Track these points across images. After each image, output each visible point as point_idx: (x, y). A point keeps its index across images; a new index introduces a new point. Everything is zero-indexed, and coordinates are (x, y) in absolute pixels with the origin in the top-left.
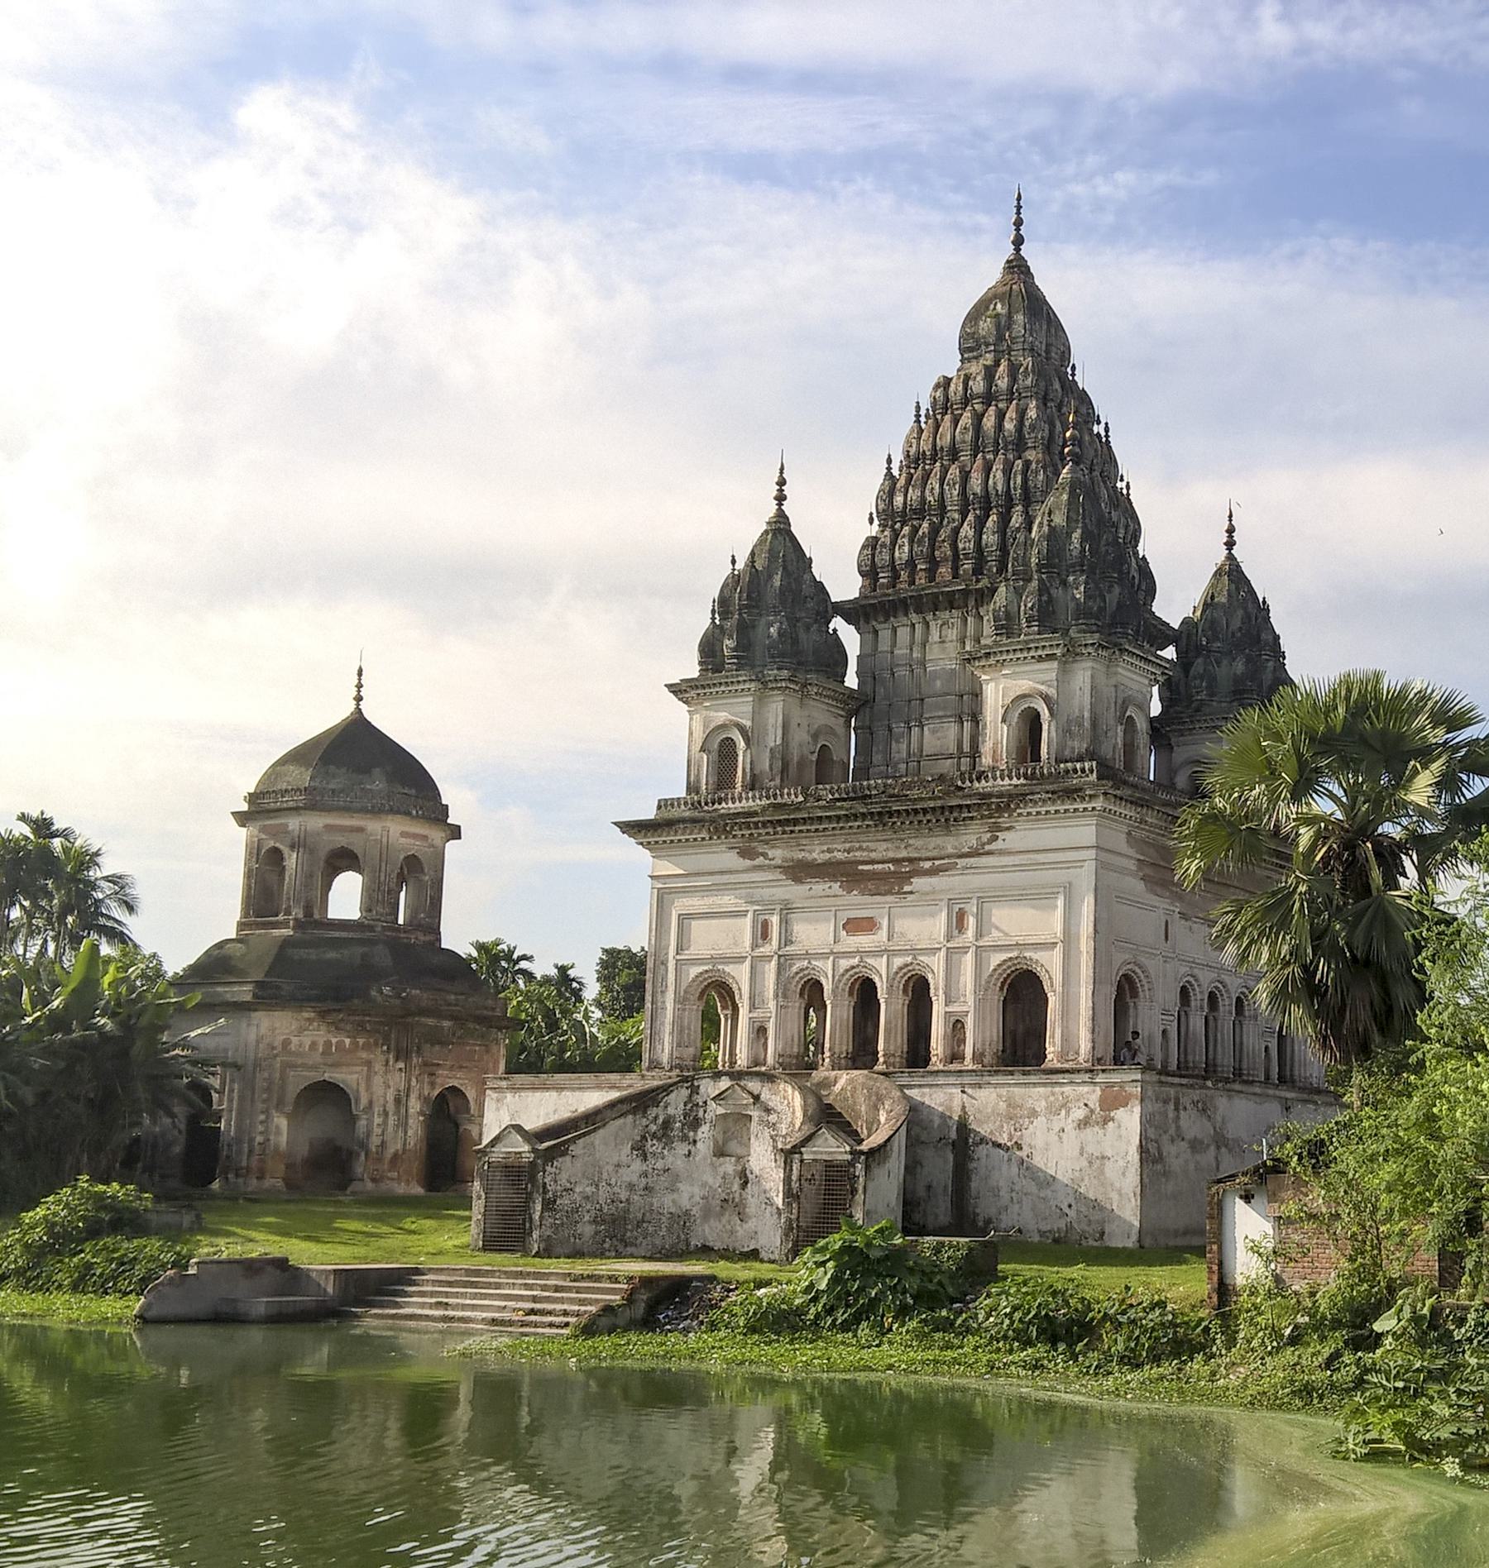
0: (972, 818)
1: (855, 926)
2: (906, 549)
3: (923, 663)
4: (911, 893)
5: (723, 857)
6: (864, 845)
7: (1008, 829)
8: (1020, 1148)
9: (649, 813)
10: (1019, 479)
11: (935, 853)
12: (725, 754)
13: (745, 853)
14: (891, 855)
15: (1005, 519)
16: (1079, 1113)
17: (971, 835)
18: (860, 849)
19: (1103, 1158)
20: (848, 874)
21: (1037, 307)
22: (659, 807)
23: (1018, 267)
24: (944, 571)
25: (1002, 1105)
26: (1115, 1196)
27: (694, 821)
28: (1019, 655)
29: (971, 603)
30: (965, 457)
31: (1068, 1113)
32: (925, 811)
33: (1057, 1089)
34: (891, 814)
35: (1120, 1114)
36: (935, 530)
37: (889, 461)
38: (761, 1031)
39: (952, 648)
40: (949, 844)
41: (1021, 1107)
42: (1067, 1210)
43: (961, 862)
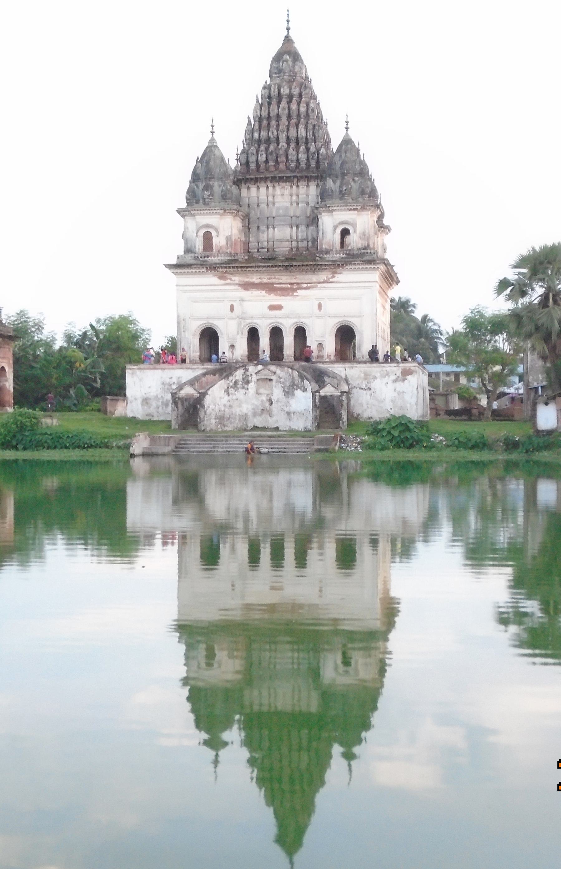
0: (325, 269)
1: (272, 308)
2: (264, 156)
3: (274, 204)
4: (298, 296)
5: (211, 279)
6: (277, 277)
7: (340, 273)
8: (370, 389)
9: (174, 261)
10: (311, 133)
11: (309, 282)
12: (208, 238)
13: (220, 278)
14: (289, 281)
15: (308, 149)
16: (394, 377)
17: (323, 276)
18: (274, 278)
19: (403, 392)
20: (269, 288)
21: (296, 57)
22: (178, 258)
23: (288, 40)
24: (282, 166)
25: (362, 375)
26: (408, 405)
27: (202, 265)
28: (341, 208)
29: (295, 180)
30: (284, 120)
31: (389, 376)
32: (307, 265)
33: (384, 369)
34: (291, 266)
35: (409, 377)
36: (277, 148)
37: (249, 118)
38: (232, 346)
39: (287, 198)
40: (314, 278)
41: (370, 375)
42: (390, 410)
43: (319, 285)
